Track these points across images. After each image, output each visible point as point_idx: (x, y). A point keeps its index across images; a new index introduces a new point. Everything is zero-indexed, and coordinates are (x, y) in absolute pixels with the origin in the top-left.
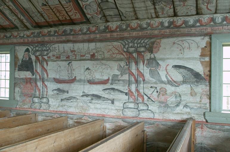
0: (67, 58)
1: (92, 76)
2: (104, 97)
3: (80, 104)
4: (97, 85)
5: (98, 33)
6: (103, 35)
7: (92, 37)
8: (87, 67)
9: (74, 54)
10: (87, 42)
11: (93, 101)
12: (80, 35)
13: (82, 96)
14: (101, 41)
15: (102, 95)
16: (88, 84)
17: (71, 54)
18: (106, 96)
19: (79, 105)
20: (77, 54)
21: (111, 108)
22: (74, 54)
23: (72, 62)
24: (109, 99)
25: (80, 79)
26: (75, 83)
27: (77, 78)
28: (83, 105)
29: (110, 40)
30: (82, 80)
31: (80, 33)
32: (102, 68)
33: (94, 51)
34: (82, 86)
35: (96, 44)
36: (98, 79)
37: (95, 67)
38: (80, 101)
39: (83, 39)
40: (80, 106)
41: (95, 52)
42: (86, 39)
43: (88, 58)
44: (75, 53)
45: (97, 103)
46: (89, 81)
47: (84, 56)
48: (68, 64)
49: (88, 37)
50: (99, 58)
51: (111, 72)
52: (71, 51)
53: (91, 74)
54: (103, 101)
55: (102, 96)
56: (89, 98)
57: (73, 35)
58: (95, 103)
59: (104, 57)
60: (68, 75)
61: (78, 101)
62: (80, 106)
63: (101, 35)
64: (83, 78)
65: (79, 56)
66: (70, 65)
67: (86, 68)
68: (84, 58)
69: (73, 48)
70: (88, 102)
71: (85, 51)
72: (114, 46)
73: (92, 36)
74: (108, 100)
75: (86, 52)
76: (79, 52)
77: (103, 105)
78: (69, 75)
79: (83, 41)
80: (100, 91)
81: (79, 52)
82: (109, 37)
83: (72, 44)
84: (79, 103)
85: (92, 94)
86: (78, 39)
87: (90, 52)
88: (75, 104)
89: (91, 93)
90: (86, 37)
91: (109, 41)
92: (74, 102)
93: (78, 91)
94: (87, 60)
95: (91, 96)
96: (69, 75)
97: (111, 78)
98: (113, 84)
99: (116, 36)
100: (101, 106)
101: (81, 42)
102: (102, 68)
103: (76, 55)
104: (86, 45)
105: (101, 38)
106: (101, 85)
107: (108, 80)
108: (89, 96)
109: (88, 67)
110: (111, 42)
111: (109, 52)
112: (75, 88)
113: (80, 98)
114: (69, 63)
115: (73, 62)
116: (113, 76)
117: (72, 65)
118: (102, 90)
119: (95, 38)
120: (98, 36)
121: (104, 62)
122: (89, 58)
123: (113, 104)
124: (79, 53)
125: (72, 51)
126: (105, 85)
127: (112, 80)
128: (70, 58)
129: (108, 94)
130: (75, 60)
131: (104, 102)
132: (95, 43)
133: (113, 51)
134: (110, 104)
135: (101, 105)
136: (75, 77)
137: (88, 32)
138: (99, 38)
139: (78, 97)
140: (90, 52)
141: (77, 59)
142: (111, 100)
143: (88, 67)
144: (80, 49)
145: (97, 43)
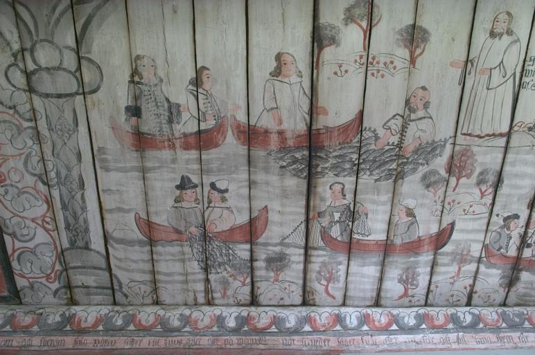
5: (37, 334)
6: (52, 341)
7: (15, 344)
63: (48, 338)
82: (71, 347)
99: (91, 346)
119: (24, 346)
138: (37, 348)
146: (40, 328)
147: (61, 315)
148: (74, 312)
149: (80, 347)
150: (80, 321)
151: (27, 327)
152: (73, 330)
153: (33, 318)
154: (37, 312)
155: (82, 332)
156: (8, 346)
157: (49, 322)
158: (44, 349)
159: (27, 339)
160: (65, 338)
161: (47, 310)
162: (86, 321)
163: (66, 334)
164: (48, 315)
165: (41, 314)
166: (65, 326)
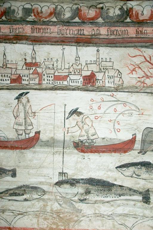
0: (13, 81)
1: (87, 132)
2: (120, 186)
3: (52, 205)
4: (101, 154)
5: (103, 25)
6: (117, 31)
7: (86, 33)
8: (75, 108)
9: (36, 73)
10: (73, 44)
11: (92, 197)
12: (54, 24)
13: (59, 184)
14: (111, 43)
15: (116, 180)
16: (76, 151)
17: (27, 72)
18: (128, 183)
19: (48, 209)
20: (44, 73)
21: (141, 214)
22: (36, 73)
23: (27, 93)
24: (135, 191)
25: (53, 139)
26: (37, 149)
27: (43, 137)
28: (59, 207)
29: (137, 44)
30: (58, 141)
31: (54, 19)
32: (115, 110)
33: (94, 68)
34: (59, 158)
35: (98, 51)
36: (103, 139)
37: (95, 106)
38: (52, 197)
39: (60, 35)
40: (52, 210)
41: (95, 70)
42: (69, 36)
43: (75, 84)
44: (39, 70)
45: (103, 202)
46: (78, 144)
47: (65, 78)
48: (18, 98)
49: (76, 32)
50: (107, 85)
51: (139, 121)
52: (26, 64)
53: (86, 127)
54: (120, 196)
55: (115, 183)
56: (80, 189)
57: (33, 23)
58: (96, 202)
59: (120, 83)
60: (16, 127)
61: (46, 197)
62: (52, 210)
63: (113, 29)
64: (59, 136)
65: (51, 79)
66: (24, 99)
67: (68, 110)
68: (65, 83)
69: (32, 58)
70: (76, 198)
71: (67, 67)
72: (148, 59)
73: (88, 31)
74: (132, 193)
75: (71, 70)
76: (49, 68)
77: (119, 206)
78: (20, 128)
79: (63, 41)
80: (110, 170)
81: (49, 68)
82: (134, 36)
83: (31, 47)
84: (49, 203)
85: (88, 177)
86: (47, 35)
87: (81, 70)
88: (38, 205)
89: (86, 175)
90: (71, 31)
91: (133, 44)
92: (33, 202)
93: (45, 171)
94: (74, 90)
95: (84, 183)
96: (20, 128)
97: (139, 137)
98: (146, 152)
100: (113, 208)
101: (55, 42)
102: (115, 110)
103: (40, 76)
104: (70, 51)
105: (112, 37)
106: (113, 154)
107: (133, 141)
108: (78, 185)
109: (77, 109)
110: (140, 48)
111: (134, 72)
112: (35, 162)
113: (51, 190)
114: (21, 95)
115: (31, 92)
116: (146, 132)
117: (28, 101)
118: (117, 168)
119: (94, 35)
120: (103, 31)
121: (120, 95)
122: (79, 84)
123: (146, 203)
124: (49, 71)
125: (29, 65)
126: (123, 154)
127: (143, 141)
128: (23, 82)
129: (132, 177)
130: (37, 87)
131: (122, 197)
132: (95, 49)
133: (146, 71)
134: (139, 204)
135: (112, 205)
136: (38, 133)
137: (77, 20)
138: (106, 37)
139: (45, 188)
140: (81, 70)
141: (44, 86)
142: (140, 193)
143: (77, 109)
144: (54, 60)
145: (100, 48)
146: (104, 20)
147: (120, 9)
148: (131, 7)
149: (142, 36)
150: (137, 15)
151: (93, 19)
152: (133, 22)
153: (96, 12)
154: (98, 6)
155: (141, 23)
156: (81, 35)
157: (111, 14)
158: (111, 37)
159: (95, 29)
160: (127, 28)
161: (107, 5)
162: (143, 14)
163: (127, 25)
164: (108, 9)
165: (102, 8)
166: (126, 19)
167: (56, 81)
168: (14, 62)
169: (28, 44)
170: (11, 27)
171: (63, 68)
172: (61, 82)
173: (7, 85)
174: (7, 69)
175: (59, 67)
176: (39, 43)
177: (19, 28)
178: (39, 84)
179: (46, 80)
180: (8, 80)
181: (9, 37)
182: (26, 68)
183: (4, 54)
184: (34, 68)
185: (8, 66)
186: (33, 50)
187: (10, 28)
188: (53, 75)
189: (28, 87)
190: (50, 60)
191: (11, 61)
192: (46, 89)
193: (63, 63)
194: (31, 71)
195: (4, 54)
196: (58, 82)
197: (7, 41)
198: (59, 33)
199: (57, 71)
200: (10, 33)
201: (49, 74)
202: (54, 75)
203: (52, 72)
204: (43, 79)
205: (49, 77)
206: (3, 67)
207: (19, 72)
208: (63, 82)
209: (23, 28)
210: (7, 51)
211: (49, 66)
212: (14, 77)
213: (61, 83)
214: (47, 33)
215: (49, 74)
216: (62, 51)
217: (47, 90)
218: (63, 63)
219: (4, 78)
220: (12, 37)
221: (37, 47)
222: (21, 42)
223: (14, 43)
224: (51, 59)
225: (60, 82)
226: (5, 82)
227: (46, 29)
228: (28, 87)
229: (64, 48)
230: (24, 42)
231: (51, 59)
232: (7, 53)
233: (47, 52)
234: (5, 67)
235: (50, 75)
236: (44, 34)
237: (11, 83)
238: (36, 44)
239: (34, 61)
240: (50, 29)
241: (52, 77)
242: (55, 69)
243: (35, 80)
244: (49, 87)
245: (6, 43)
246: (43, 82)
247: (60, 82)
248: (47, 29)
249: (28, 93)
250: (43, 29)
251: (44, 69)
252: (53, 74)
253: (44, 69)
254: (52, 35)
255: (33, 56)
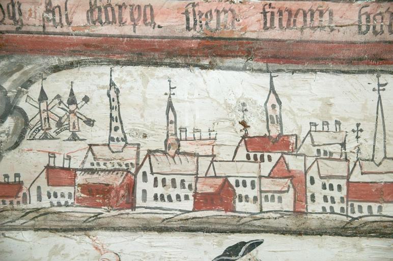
0: (203, 201)
9: (281, 172)
17: (249, 170)
20: (313, 172)
22: (281, 172)
23: (255, 244)
39: (369, 36)
44: (295, 164)
52: (248, 141)
65: (337, 195)
69: (269, 120)
76: (329, 156)
81: (329, 156)
83: (264, 79)
86: (318, 35)
101: (350, 61)
103: (298, 182)
124: (328, 167)
128: (240, 206)
130: (289, 222)
141: (313, 222)
167: (356, 204)
168: (205, 135)
169: (252, 70)
170: (190, 9)
171: (379, 156)
172: (375, 207)
173: (183, 216)
174: (182, 157)
175: (366, 153)
176: (293, 67)
177: (218, 11)
178: (298, 213)
179: (319, 199)
180: (187, 197)
181: (185, 45)
182: (248, 157)
183: (170, 106)
184: (276, 156)
185: (185, 147)
186: (272, 89)
187: (187, 13)
188: (343, 183)
189: (257, 223)
190: (332, 127)
191: (196, 130)
192: (320, 232)
193: (380, 136)
194: (267, 168)
195: (170, 106)
196: (365, 205)
197: (180, 61)
198: (364, 28)
199: (358, 167)
200: (188, 28)
201: (331, 177)
202: (348, 183)
203: (340, 168)
204: (309, 194)
205: (331, 187)
206: (165, 153)
207: (222, 170)
208: (380, 208)
209: (232, 11)
210: (179, 94)
211: (328, 148)
212: (205, 188)
213: (375, 211)
214: (322, 27)
215: (331, 177)
216: (376, 94)
217: (326, 233)
218: (380, 136)
219: (173, 193)
220: (194, 44)
221: (285, 81)
222: (229, 62)
223: (203, 67)
224: (338, 123)
225: (370, 208)
226: (175, 205)
227: (316, 15)
228: (257, 223)
229: (382, 81)
230: (240, 61)
231: (338, 123)
232: (178, 101)
233: (320, 99)
234: (172, 151)
235: (335, 183)
236: (307, 35)
237: (197, 207)
238: (279, 71)
239: (274, 132)
240: (331, 14)
241: (339, 187)
242: (353, 158)
243: (280, 199)
244: (332, 224)
245: (177, 65)
246: (311, 207)
247: (370, 208)
248: (321, 14)
249: (259, 243)
250: (305, 15)
251: (310, 161)
252: (342, 177)
253: (310, 161)
254: (340, 36)
255: (270, 112)
